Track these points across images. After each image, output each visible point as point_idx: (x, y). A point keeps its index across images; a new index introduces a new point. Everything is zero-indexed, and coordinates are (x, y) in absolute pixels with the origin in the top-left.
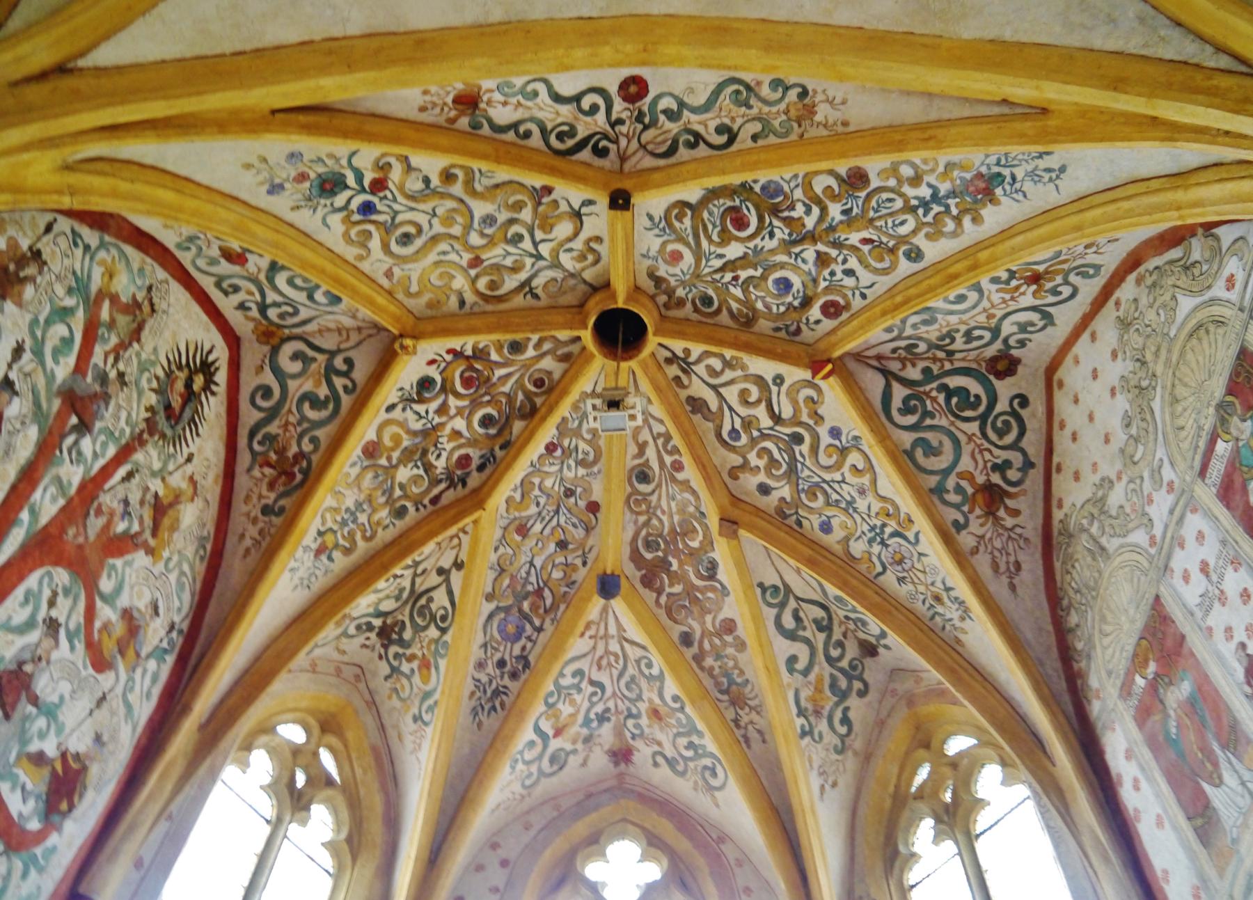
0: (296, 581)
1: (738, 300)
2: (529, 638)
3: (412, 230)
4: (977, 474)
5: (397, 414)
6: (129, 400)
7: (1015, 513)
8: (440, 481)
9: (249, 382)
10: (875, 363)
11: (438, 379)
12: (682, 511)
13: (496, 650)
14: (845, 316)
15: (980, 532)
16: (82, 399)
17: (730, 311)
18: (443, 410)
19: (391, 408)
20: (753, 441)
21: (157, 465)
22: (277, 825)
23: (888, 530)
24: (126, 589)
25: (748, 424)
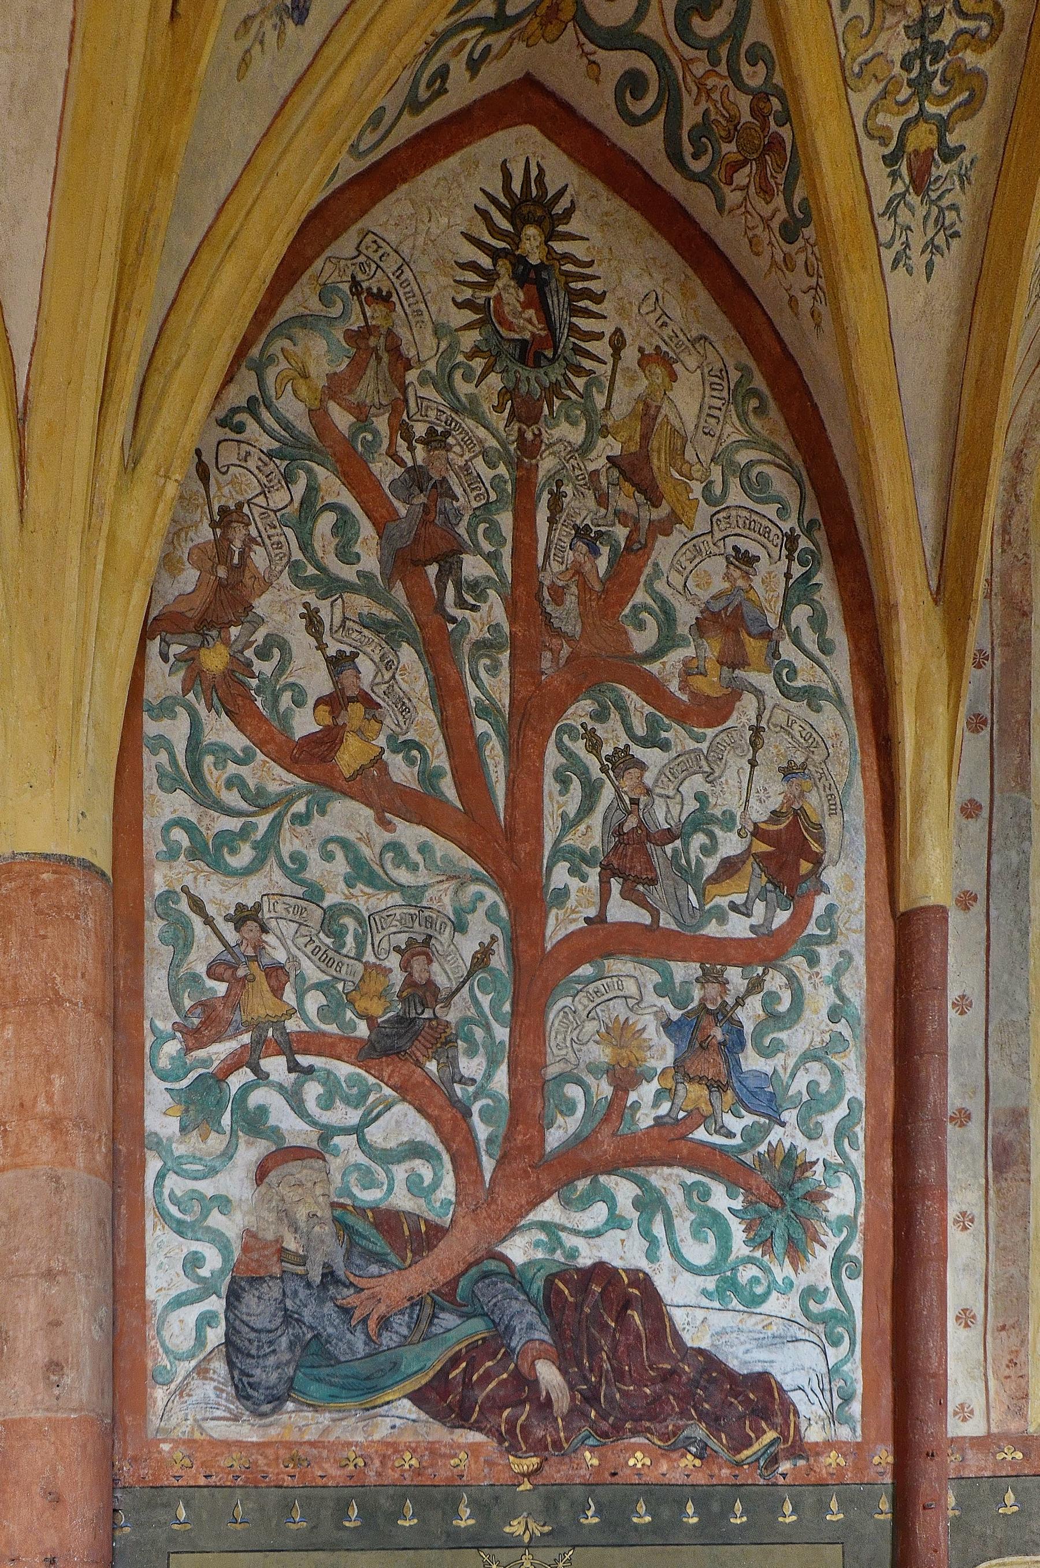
6: (469, 441)
16: (416, 540)
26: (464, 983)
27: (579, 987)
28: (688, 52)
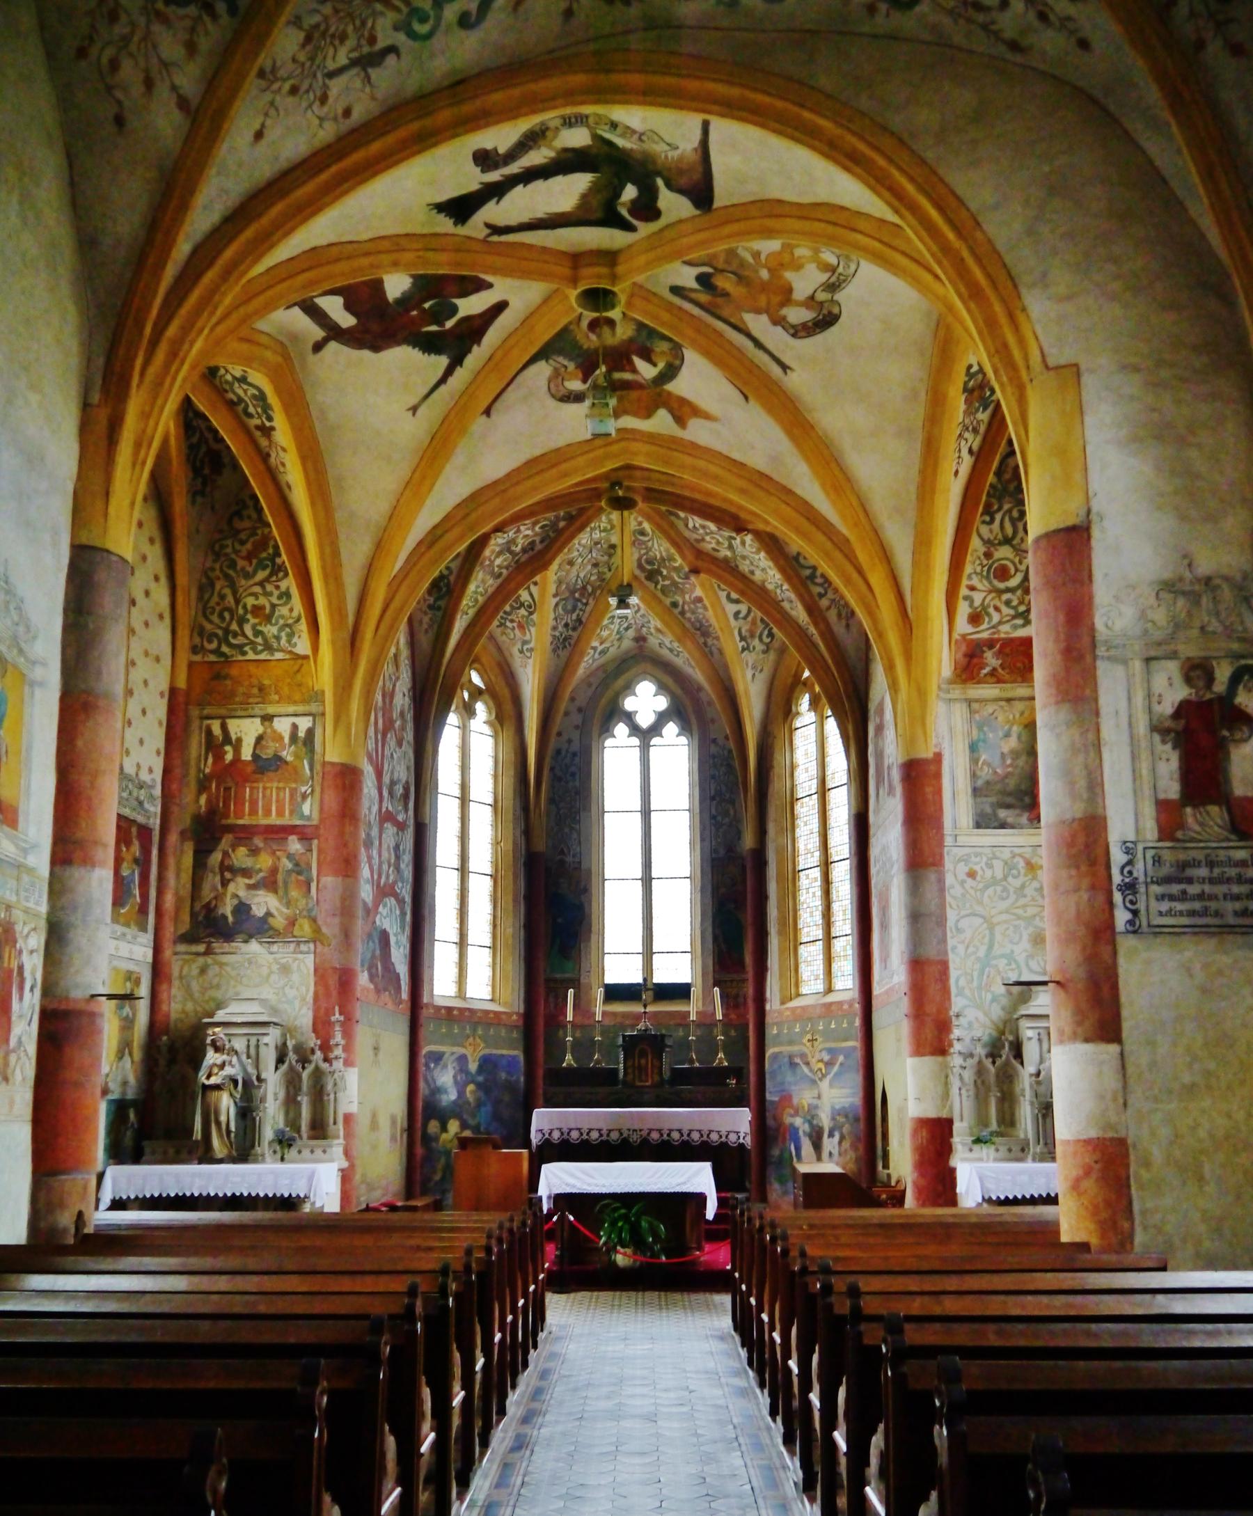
20: (707, 534)
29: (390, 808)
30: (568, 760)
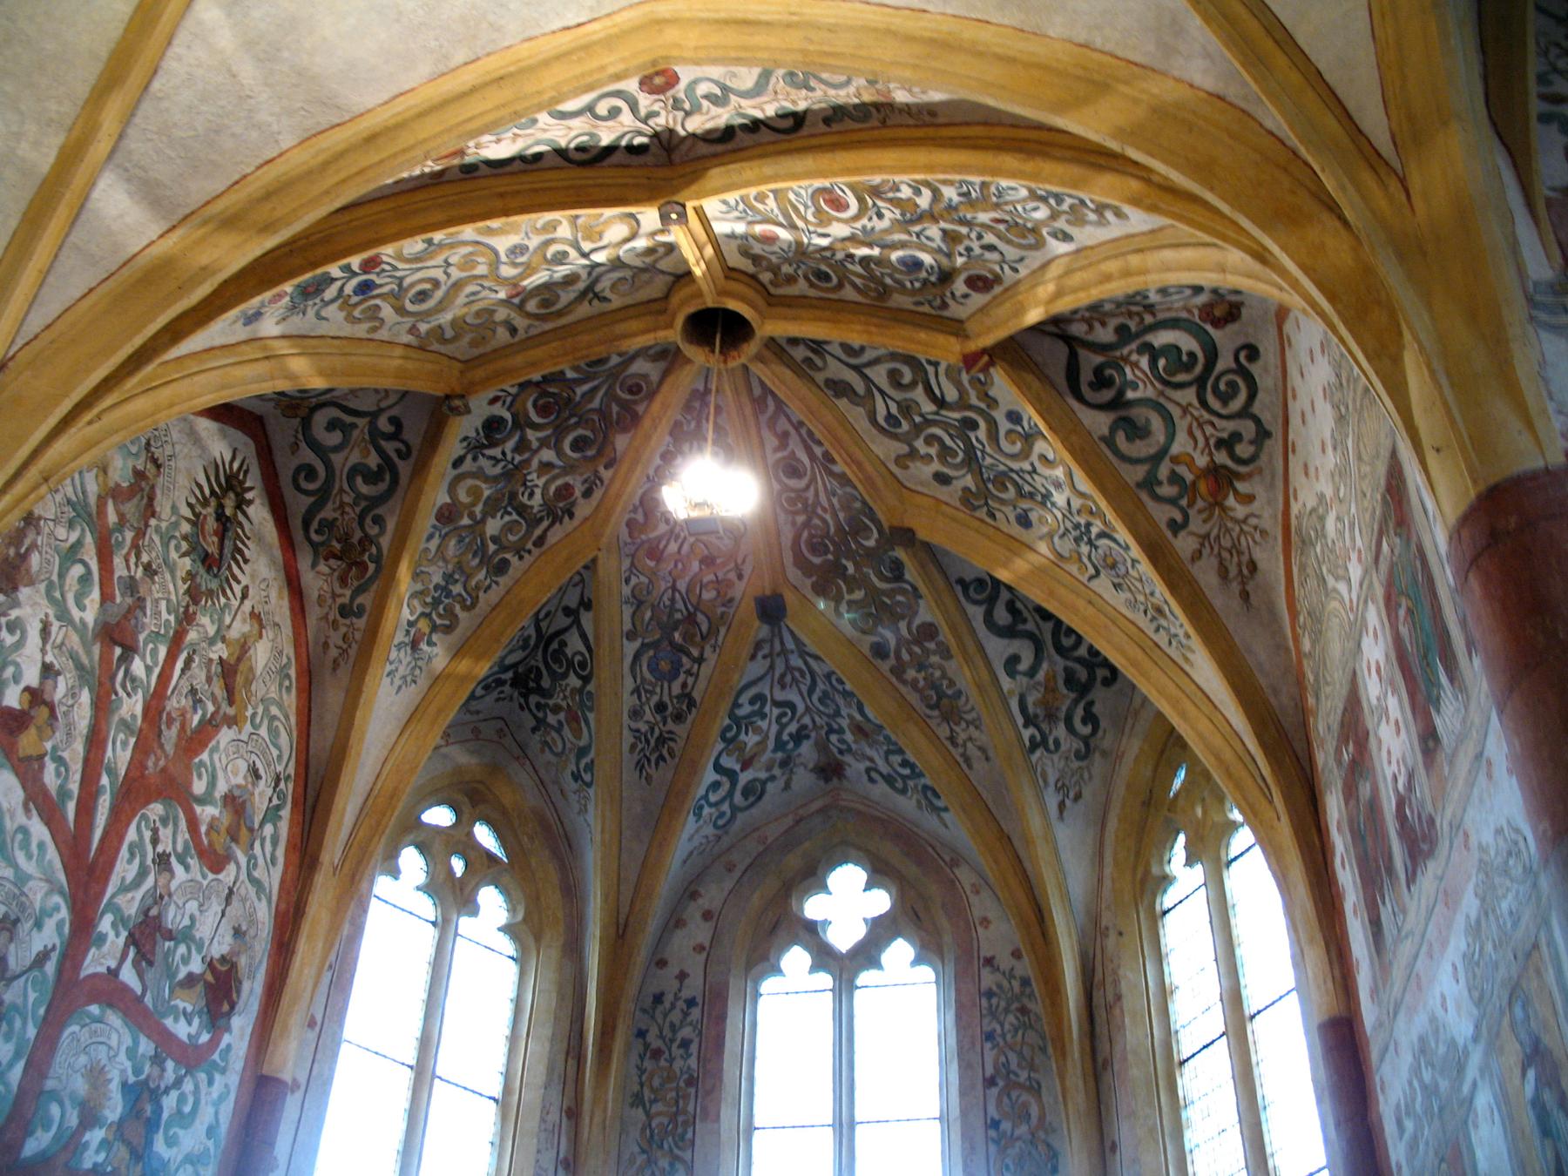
0: (397, 682)
1: (859, 276)
2: (688, 673)
3: (427, 286)
4: (1196, 455)
5: (468, 465)
6: (164, 586)
7: (1249, 499)
8: (541, 519)
9: (286, 465)
10: (1052, 329)
11: (508, 416)
12: (846, 507)
13: (652, 693)
14: (997, 290)
15: (1203, 530)
16: (118, 624)
17: (854, 285)
18: (523, 445)
19: (457, 463)
20: (917, 429)
21: (211, 630)
22: (444, 925)
23: (1094, 530)
24: (220, 774)
25: (907, 408)
26: (24, 973)
27: (88, 1021)
28: (346, 486)
29: (128, 975)
30: (676, 1016)
